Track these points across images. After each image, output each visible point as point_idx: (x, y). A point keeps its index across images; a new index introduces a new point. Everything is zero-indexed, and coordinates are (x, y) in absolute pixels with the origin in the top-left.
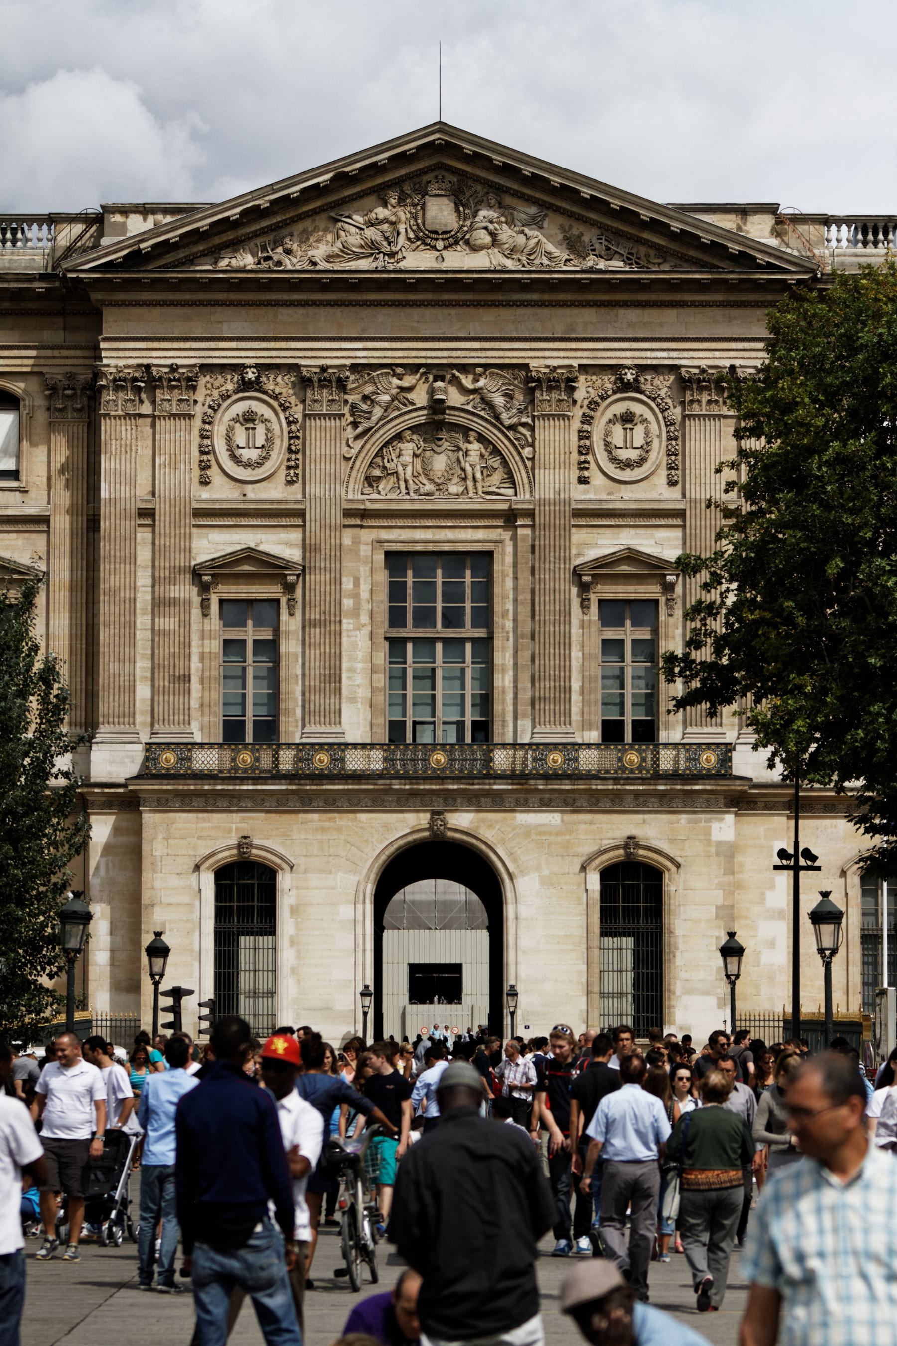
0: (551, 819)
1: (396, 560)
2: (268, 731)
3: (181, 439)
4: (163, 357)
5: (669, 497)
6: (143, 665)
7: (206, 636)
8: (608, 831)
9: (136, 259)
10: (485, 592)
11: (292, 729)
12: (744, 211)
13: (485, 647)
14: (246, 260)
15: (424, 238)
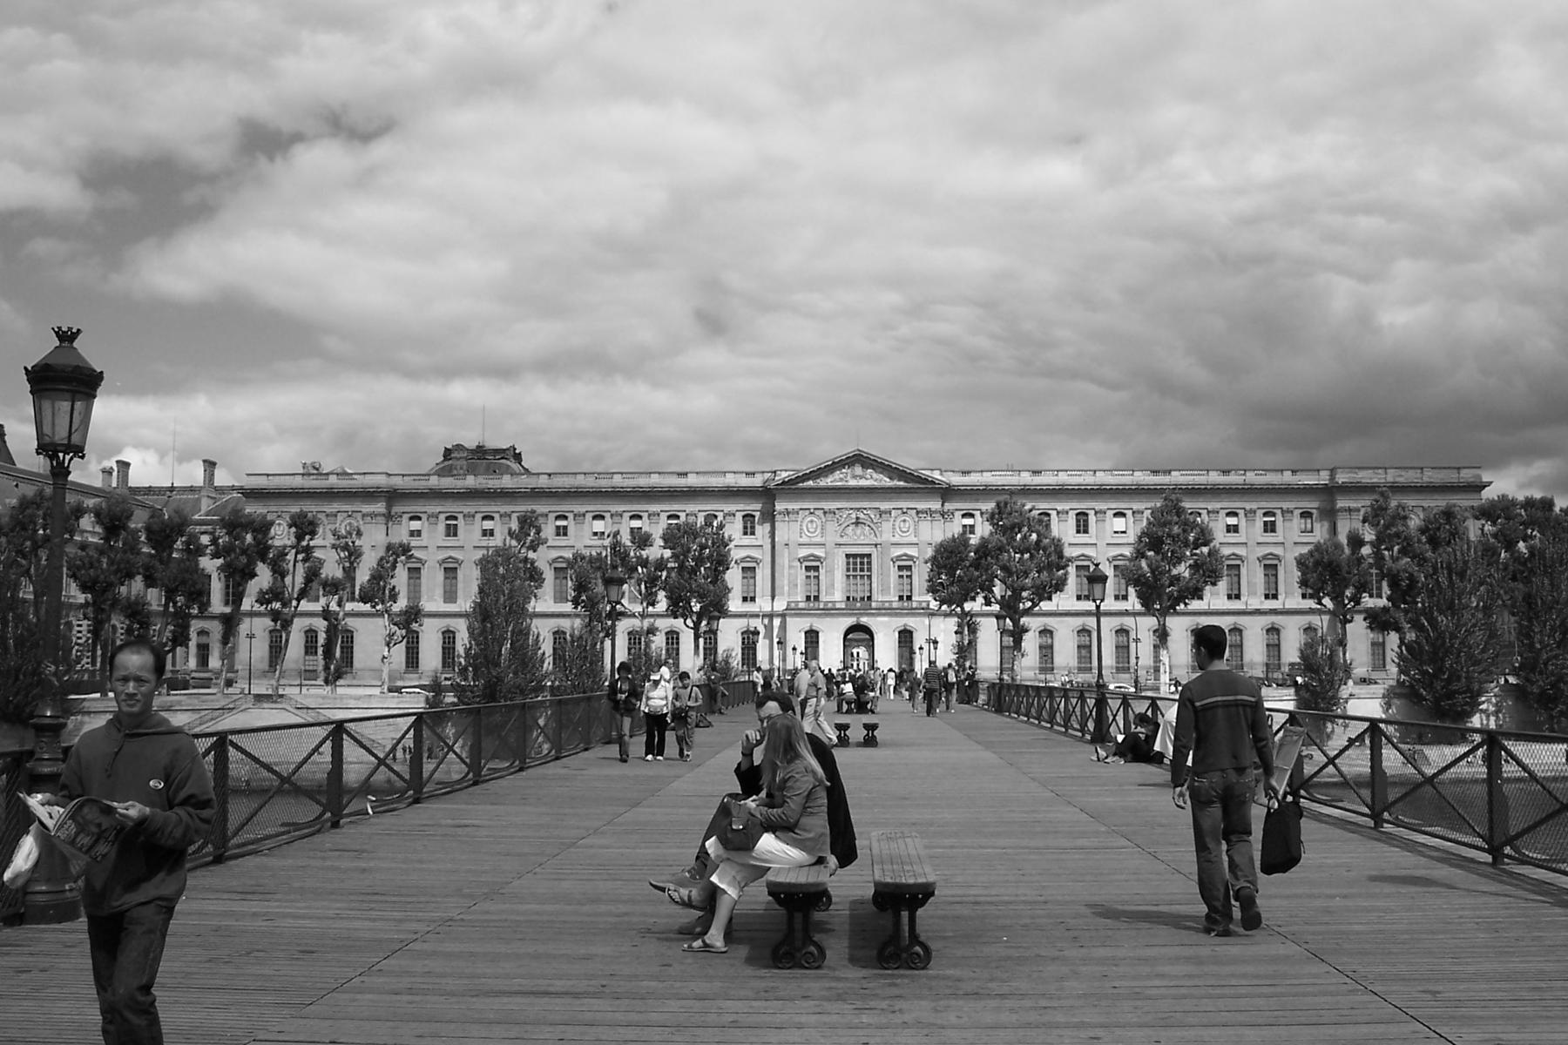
0: (886, 619)
1: (848, 556)
2: (817, 598)
3: (795, 527)
5: (915, 540)
7: (802, 574)
8: (901, 622)
9: (784, 483)
10: (869, 563)
11: (823, 598)
13: (870, 577)
14: (811, 483)
15: (854, 477)
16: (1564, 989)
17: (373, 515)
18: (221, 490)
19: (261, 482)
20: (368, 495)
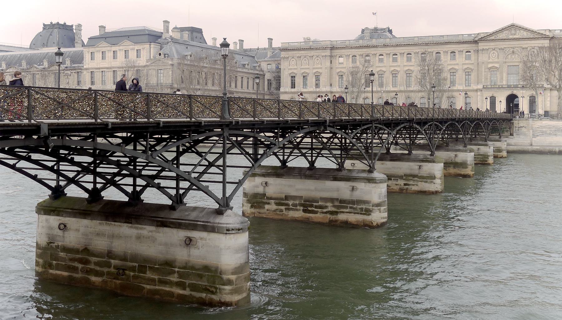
4: (485, 48)
6: (483, 77)
12: (546, 30)
15: (512, 34)
16: (561, 265)
17: (326, 56)
18: (273, 49)
19: (286, 46)
20: (325, 49)
